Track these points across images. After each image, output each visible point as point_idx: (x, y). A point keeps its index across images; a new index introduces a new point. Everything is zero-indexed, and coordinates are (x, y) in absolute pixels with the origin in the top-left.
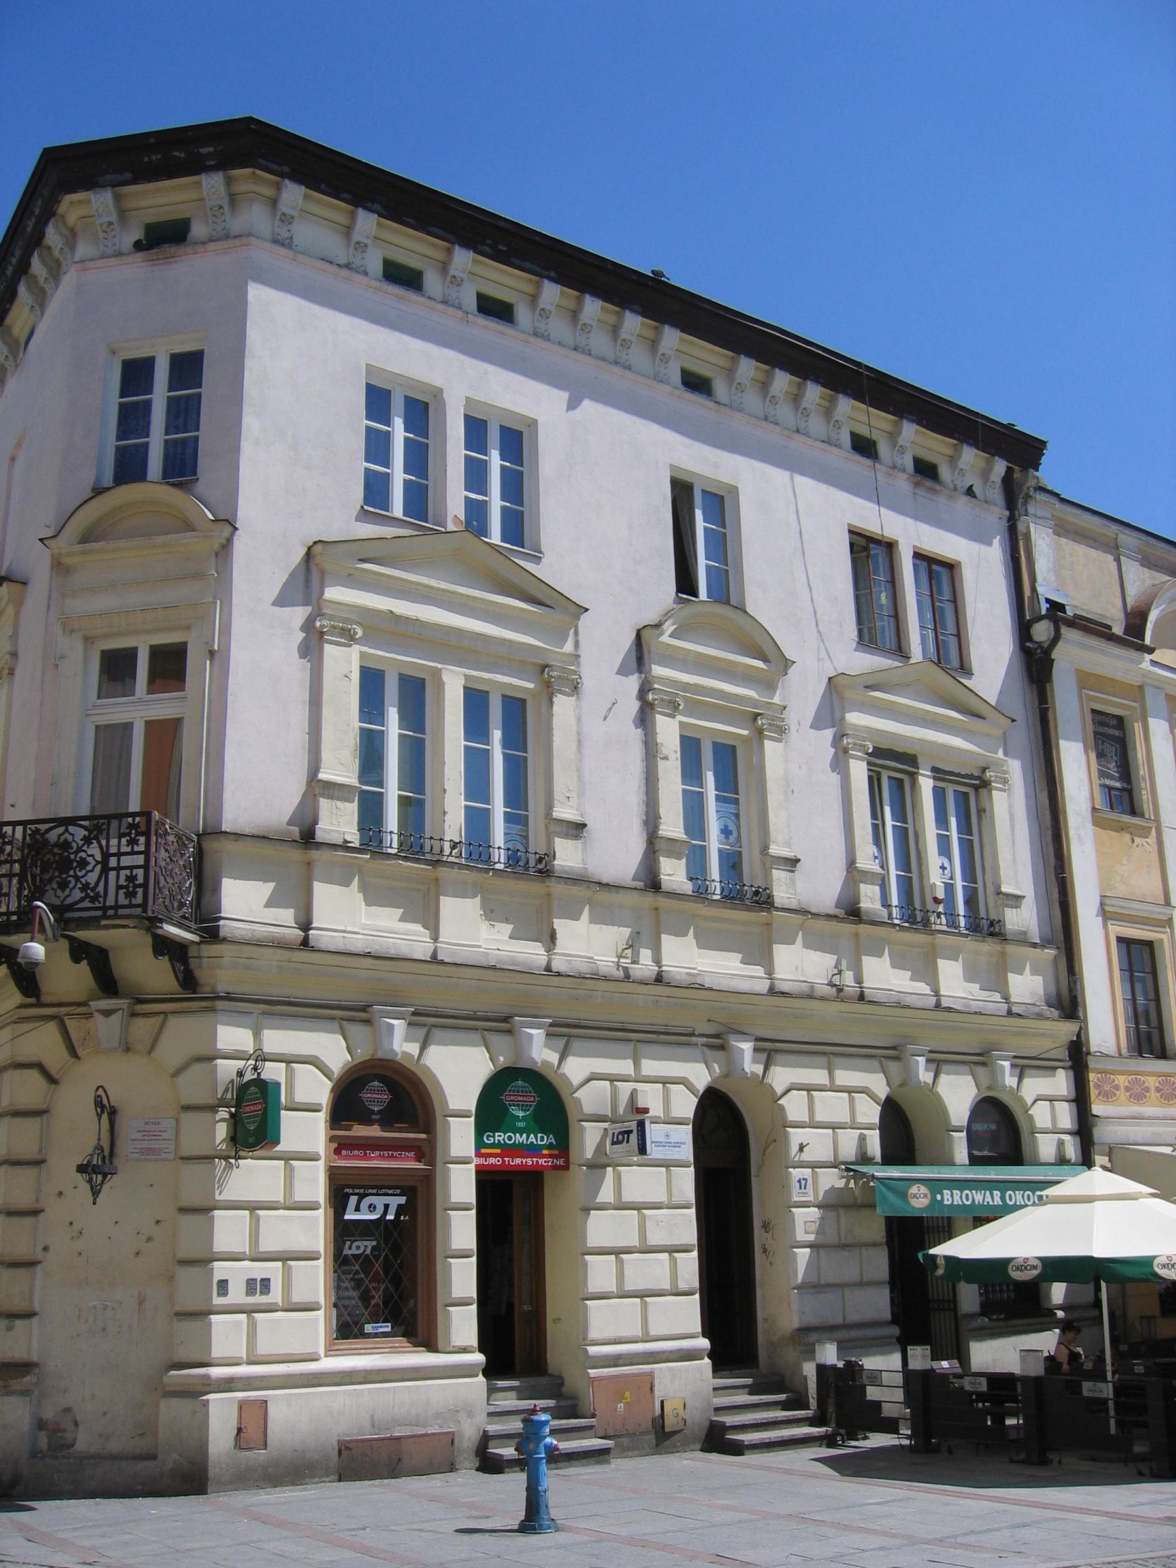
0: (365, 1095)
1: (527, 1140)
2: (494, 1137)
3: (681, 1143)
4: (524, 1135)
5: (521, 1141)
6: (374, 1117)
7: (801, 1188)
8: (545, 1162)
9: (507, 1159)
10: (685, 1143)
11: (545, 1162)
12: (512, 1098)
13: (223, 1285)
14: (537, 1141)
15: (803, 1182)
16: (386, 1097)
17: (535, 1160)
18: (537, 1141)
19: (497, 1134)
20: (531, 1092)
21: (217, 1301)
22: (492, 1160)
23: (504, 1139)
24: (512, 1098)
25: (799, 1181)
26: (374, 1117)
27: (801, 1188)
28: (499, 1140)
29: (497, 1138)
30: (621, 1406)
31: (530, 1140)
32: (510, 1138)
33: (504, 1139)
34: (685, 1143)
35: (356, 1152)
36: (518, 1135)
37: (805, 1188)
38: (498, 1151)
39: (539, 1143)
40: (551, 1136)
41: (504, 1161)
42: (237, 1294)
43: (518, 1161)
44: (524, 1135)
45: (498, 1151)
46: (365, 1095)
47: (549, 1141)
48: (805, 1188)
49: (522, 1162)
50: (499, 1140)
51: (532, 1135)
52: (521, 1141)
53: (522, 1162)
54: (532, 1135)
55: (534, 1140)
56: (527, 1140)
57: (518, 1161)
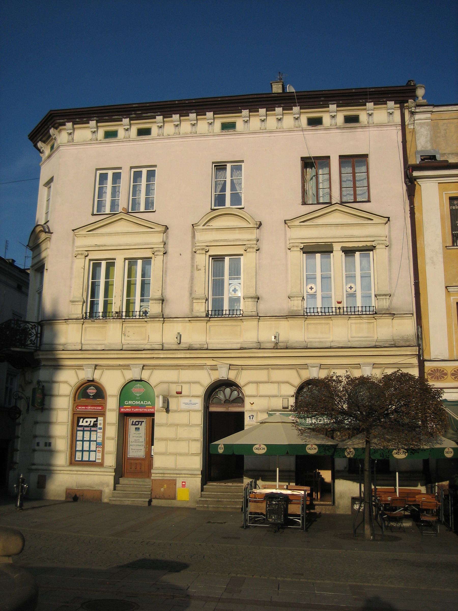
0: (88, 391)
1: (140, 403)
2: (128, 402)
3: (196, 403)
4: (139, 402)
5: (138, 403)
6: (91, 397)
7: (250, 419)
8: (147, 410)
9: (133, 409)
10: (198, 403)
11: (147, 410)
12: (135, 390)
13: (38, 444)
14: (144, 403)
15: (251, 417)
16: (95, 391)
17: (143, 409)
18: (144, 403)
19: (129, 401)
20: (142, 388)
21: (37, 448)
22: (127, 410)
23: (132, 403)
24: (135, 390)
25: (250, 417)
26: (91, 397)
27: (250, 419)
28: (130, 403)
29: (129, 403)
30: (162, 489)
31: (141, 403)
32: (134, 403)
33: (132, 403)
34: (198, 403)
35: (83, 408)
36: (137, 402)
37: (252, 419)
38: (130, 407)
39: (145, 404)
40: (149, 402)
41: (132, 410)
42: (42, 446)
43: (137, 410)
44: (139, 402)
45: (130, 407)
46: (88, 391)
47: (148, 403)
48: (252, 419)
49: (138, 410)
50: (130, 403)
51: (142, 402)
52: (138, 403)
53: (138, 410)
54: (142, 402)
55: (143, 403)
56: (140, 403)
57: (137, 410)
